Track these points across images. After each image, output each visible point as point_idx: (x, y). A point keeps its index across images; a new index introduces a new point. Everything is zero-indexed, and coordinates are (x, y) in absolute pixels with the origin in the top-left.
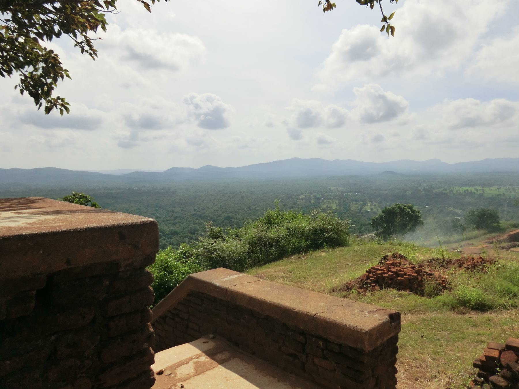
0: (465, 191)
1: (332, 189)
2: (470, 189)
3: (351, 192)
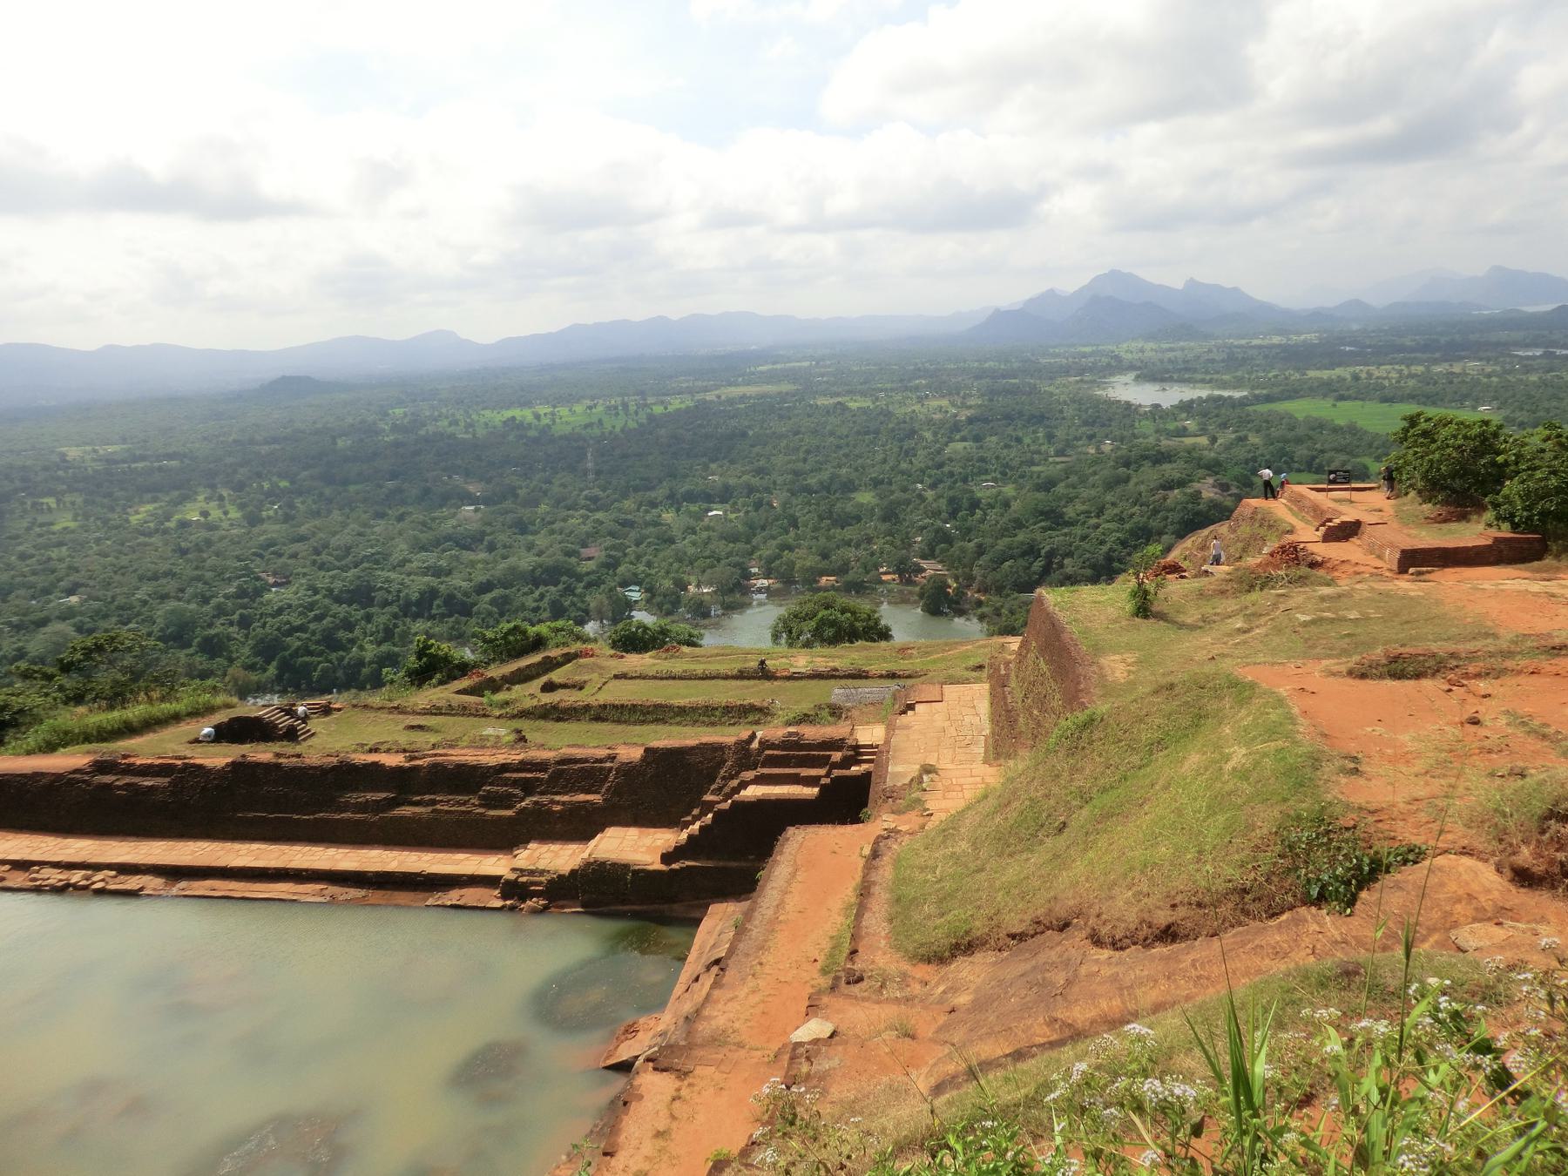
1: (73, 453)
2: (517, 413)
3: (143, 458)
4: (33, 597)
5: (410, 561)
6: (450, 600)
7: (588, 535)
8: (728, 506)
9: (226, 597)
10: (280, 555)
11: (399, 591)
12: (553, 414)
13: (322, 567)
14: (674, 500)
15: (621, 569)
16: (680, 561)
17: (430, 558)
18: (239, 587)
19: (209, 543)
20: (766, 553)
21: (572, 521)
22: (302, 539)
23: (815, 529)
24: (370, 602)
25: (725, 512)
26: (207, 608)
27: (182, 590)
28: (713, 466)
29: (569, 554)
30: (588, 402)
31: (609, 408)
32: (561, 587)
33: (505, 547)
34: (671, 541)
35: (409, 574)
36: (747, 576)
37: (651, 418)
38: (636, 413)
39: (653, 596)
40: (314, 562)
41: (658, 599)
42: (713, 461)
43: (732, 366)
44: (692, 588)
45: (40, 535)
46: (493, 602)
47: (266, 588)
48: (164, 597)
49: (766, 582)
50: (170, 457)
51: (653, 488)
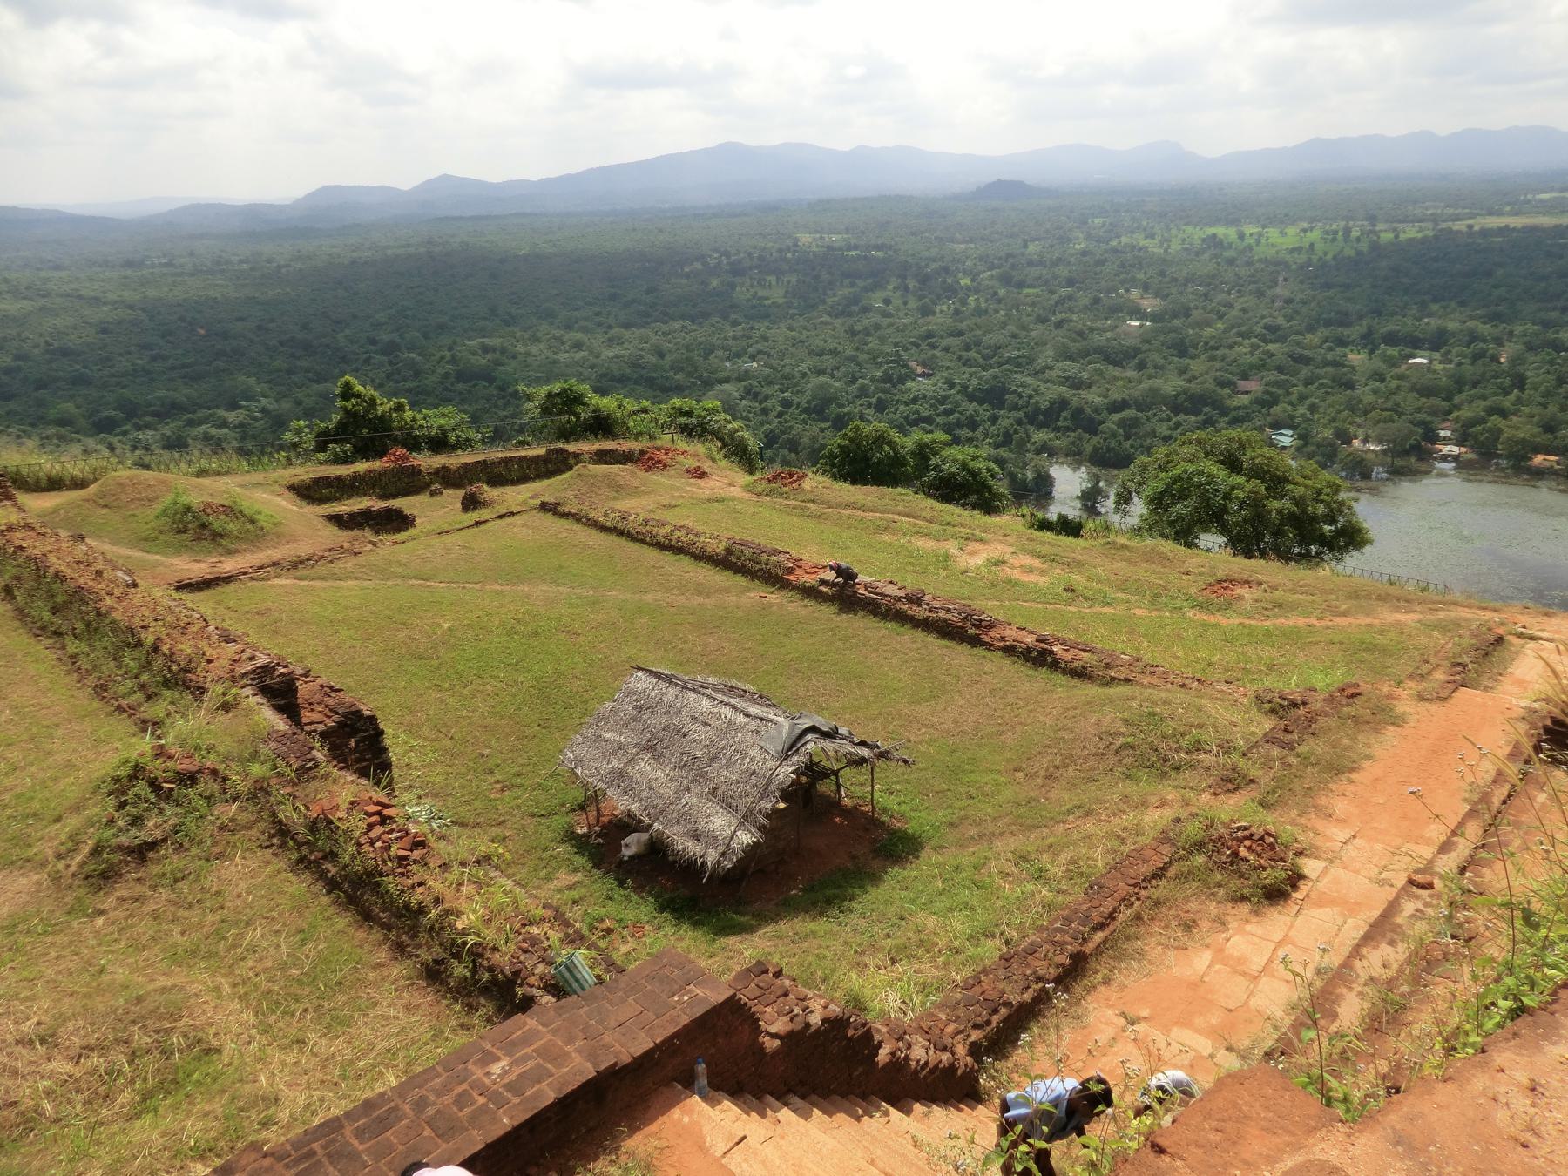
0: (1204, 240)
1: (805, 239)
2: (1220, 231)
3: (856, 247)
4: (728, 359)
5: (1051, 368)
6: (1079, 411)
7: (1252, 367)
8: (1437, 355)
9: (873, 380)
10: (933, 346)
11: (1031, 397)
12: (1260, 235)
13: (967, 363)
14: (1369, 342)
15: (1276, 409)
16: (1353, 410)
17: (1072, 368)
18: (885, 372)
19: (877, 327)
20: (1466, 413)
21: (1238, 349)
22: (960, 334)
23: (1548, 394)
24: (1001, 404)
25: (1431, 361)
26: (853, 388)
27: (838, 369)
28: (1435, 307)
29: (1222, 384)
30: (1305, 225)
31: (1327, 233)
32: (1201, 418)
33: (1156, 367)
34: (1350, 385)
35: (1047, 381)
36: (1432, 437)
37: (1375, 246)
38: (1358, 240)
39: (1306, 444)
40: (960, 358)
41: (1311, 448)
42: (1435, 300)
43: (1505, 194)
44: (1356, 443)
45: (754, 307)
46: (1121, 423)
47: (912, 376)
48: (821, 372)
49: (1456, 450)
50: (878, 248)
51: (1349, 325)
